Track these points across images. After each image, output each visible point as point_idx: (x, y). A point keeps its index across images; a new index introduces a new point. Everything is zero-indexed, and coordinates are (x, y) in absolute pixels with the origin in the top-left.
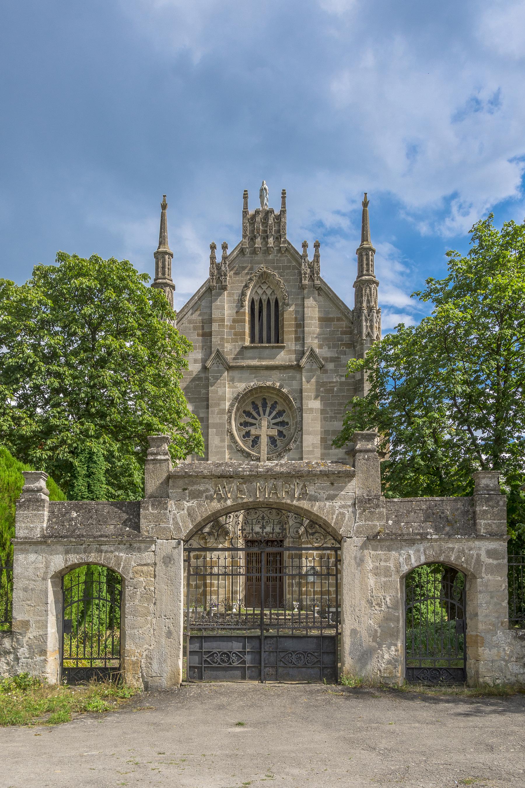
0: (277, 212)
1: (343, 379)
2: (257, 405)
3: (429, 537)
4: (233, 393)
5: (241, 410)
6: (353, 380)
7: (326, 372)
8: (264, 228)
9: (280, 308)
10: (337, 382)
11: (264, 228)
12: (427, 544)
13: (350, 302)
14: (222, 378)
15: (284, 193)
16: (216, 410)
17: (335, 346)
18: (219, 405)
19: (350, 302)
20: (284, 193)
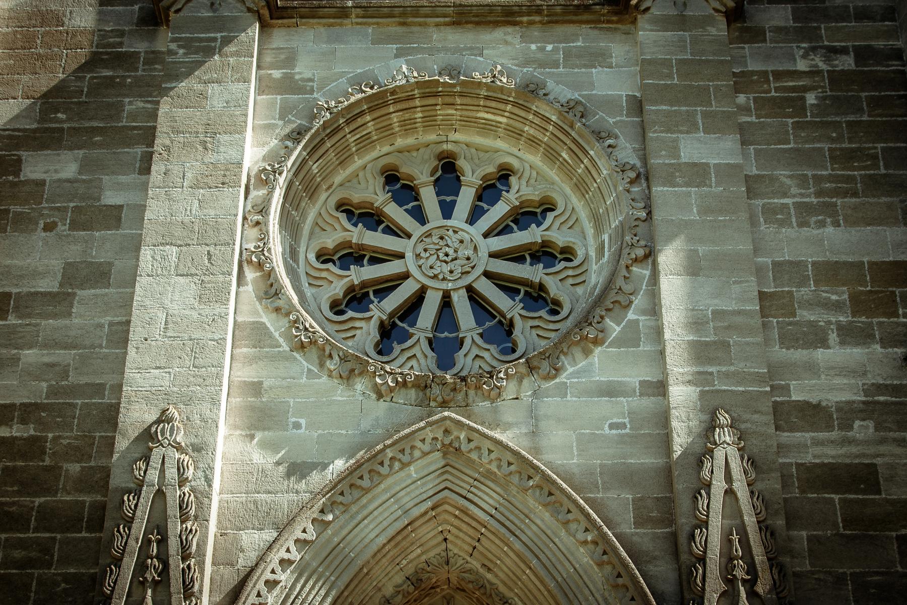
1: (847, 63)
5: (325, 201)
7: (755, 35)
10: (814, 73)
14: (231, 48)
16: (192, 168)
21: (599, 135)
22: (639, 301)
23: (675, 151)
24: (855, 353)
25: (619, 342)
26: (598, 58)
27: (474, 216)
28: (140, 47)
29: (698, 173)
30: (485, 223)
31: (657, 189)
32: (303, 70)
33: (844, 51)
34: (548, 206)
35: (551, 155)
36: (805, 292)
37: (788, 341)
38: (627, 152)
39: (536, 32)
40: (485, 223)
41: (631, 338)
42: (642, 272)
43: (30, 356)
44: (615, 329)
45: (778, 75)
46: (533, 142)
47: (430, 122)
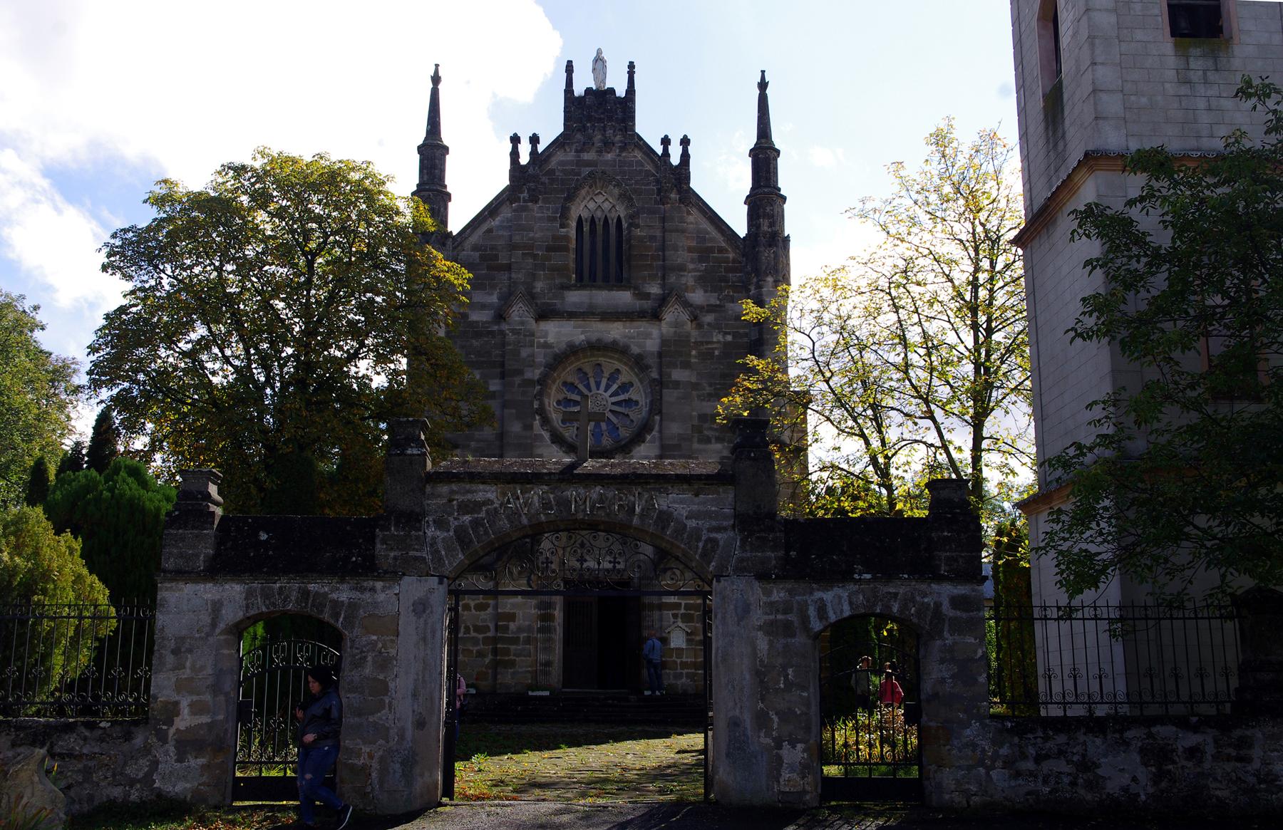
0: (621, 91)
1: (729, 338)
2: (586, 374)
3: (856, 576)
4: (545, 356)
6: (746, 340)
8: (599, 115)
9: (625, 233)
10: (719, 342)
11: (599, 115)
12: (853, 587)
13: (739, 223)
15: (631, 66)
16: (517, 380)
17: (714, 290)
18: (520, 372)
19: (739, 223)
20: (631, 66)
21: (647, 367)
22: (657, 428)
23: (670, 376)
24: (719, 446)
25: (651, 442)
26: (648, 335)
27: (607, 388)
28: (496, 328)
29: (677, 384)
30: (610, 392)
31: (665, 391)
32: (551, 339)
33: (726, 333)
34: (631, 384)
35: (632, 368)
36: (706, 425)
37: (700, 441)
38: (655, 375)
39: (628, 324)
40: (610, 392)
41: (652, 442)
42: (657, 418)
43: (473, 444)
44: (649, 437)
45: (708, 343)
46: (626, 364)
47: (592, 356)
